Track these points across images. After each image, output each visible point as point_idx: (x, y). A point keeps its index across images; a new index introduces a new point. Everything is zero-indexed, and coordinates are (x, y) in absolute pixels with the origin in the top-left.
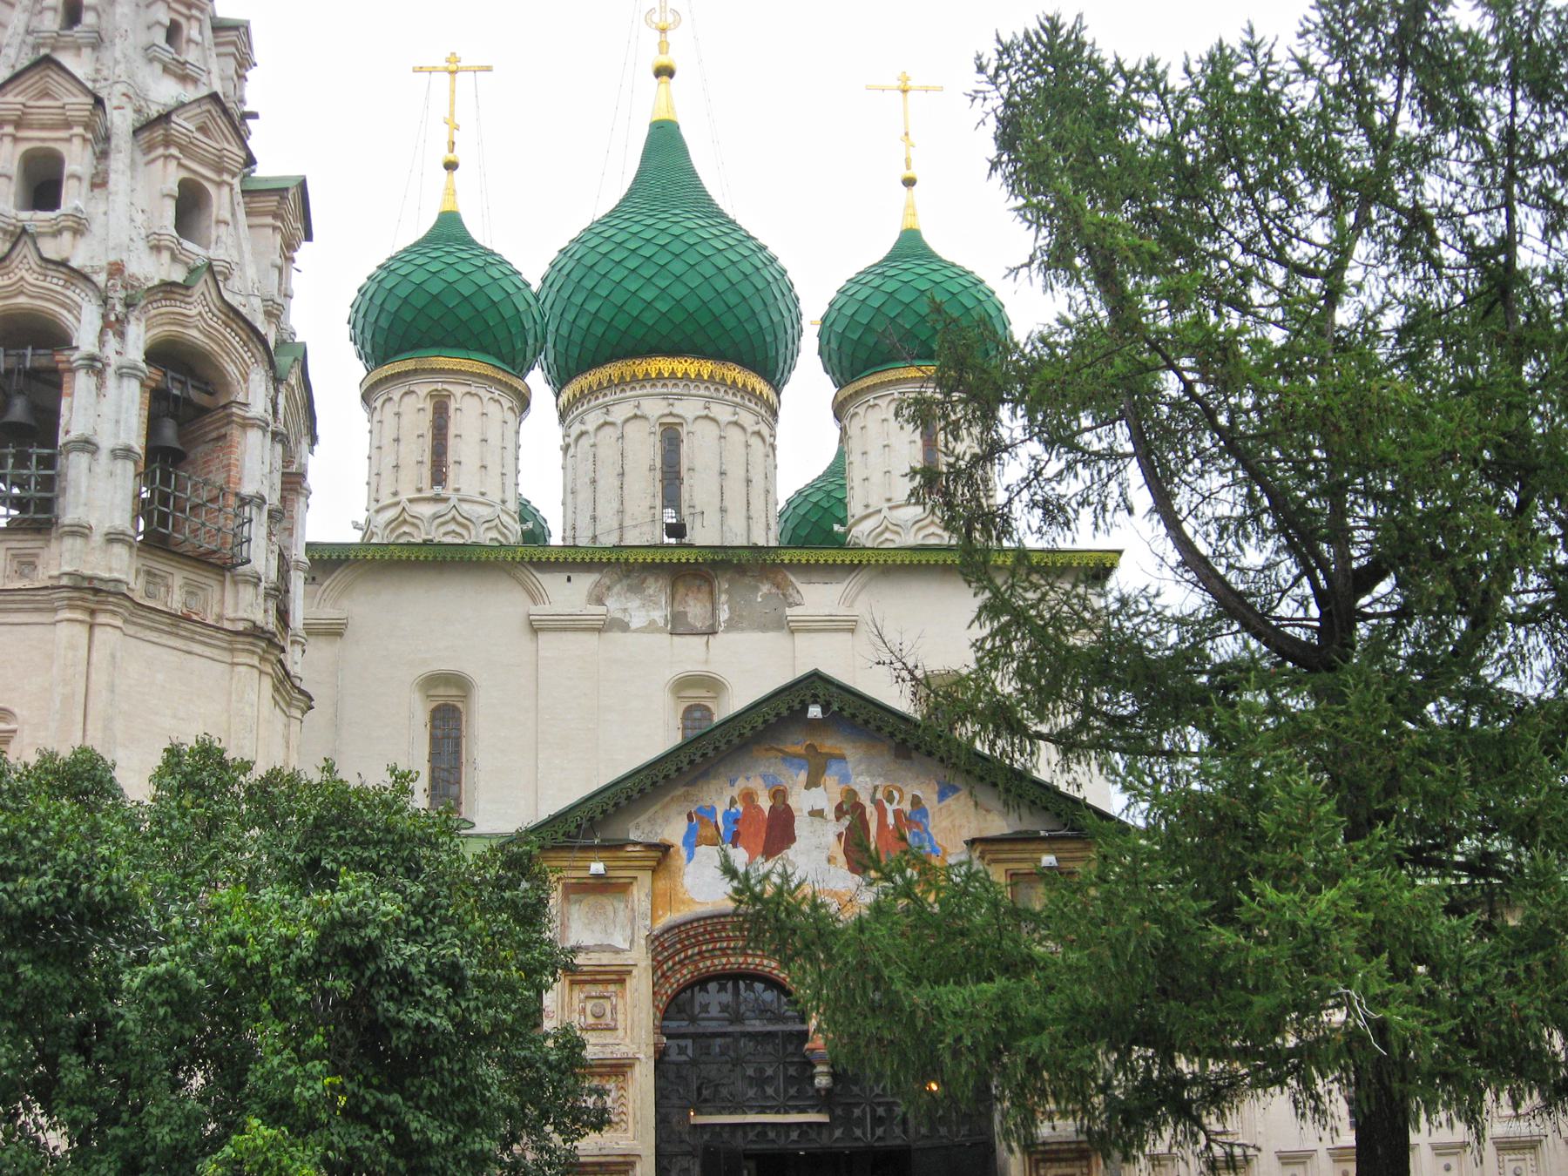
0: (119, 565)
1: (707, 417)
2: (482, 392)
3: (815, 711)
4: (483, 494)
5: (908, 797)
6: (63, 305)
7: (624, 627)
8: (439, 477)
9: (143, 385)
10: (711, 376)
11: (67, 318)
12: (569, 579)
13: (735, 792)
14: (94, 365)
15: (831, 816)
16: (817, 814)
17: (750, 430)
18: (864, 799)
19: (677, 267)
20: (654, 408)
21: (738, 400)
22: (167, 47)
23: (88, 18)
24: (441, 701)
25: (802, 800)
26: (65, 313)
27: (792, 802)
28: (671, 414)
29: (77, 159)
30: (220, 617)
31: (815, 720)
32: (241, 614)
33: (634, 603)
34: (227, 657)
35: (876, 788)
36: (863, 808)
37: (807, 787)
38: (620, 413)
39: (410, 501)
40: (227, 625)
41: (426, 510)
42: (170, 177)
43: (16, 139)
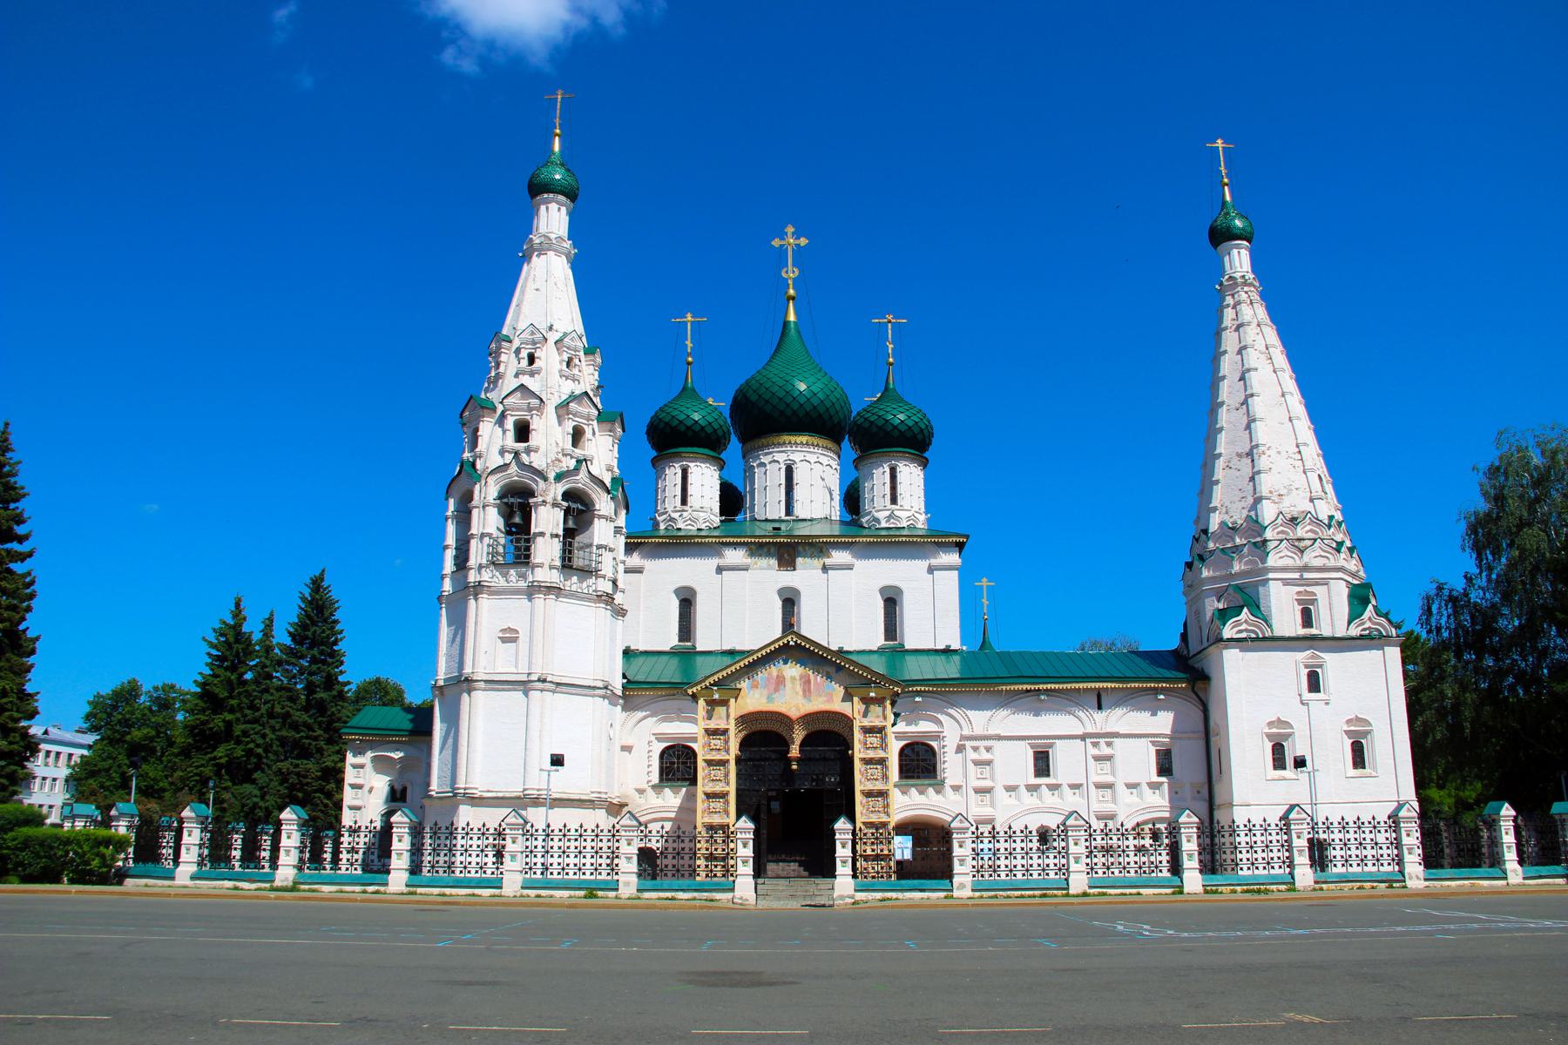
0: (554, 577)
4: (702, 508)
8: (684, 501)
15: (798, 678)
16: (793, 679)
17: (825, 464)
20: (781, 457)
22: (567, 370)
27: (785, 674)
37: (790, 668)
42: (569, 426)
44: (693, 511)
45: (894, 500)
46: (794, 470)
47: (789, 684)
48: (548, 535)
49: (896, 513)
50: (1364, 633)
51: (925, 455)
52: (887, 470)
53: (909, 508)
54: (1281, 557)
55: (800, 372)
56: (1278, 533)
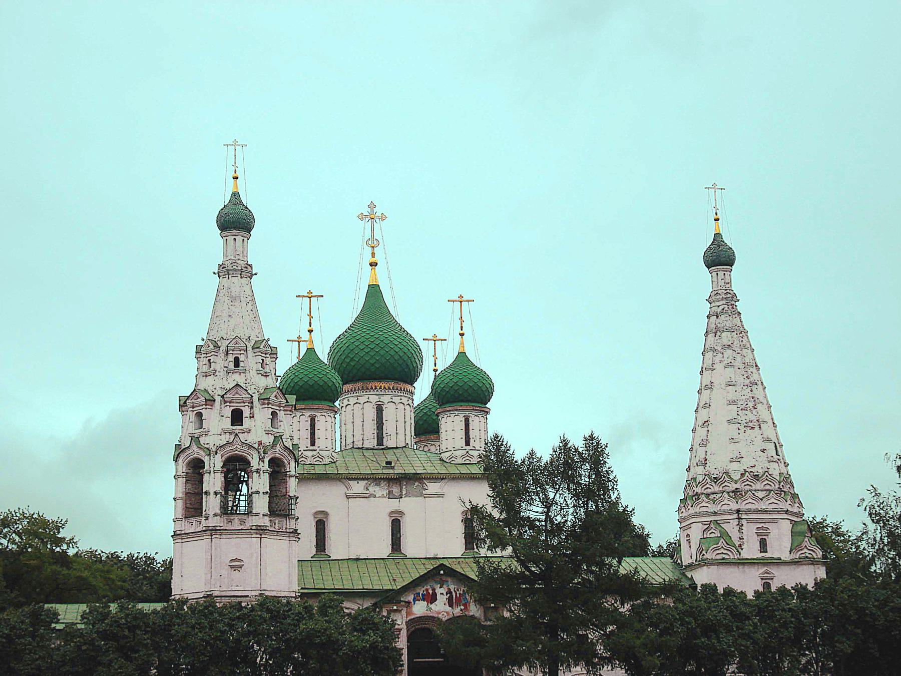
0: (266, 521)
1: (392, 402)
2: (325, 414)
3: (442, 572)
5: (462, 590)
6: (248, 454)
7: (375, 496)
8: (313, 444)
9: (269, 473)
10: (393, 388)
11: (249, 458)
12: (358, 483)
13: (424, 589)
14: (258, 471)
15: (445, 594)
18: (452, 590)
19: (382, 352)
20: (374, 399)
21: (402, 394)
23: (241, 364)
24: (318, 519)
25: (439, 591)
26: (248, 456)
28: (380, 401)
29: (246, 412)
30: (286, 528)
31: (442, 574)
32: (291, 527)
33: (377, 488)
34: (288, 539)
35: (455, 588)
36: (452, 592)
38: (362, 400)
39: (304, 450)
40: (288, 531)
41: (309, 454)
43: (230, 406)
44: (320, 450)
45: (467, 443)
46: (384, 408)
47: (438, 596)
48: (261, 493)
49: (470, 452)
50: (801, 556)
51: (487, 406)
52: (463, 419)
53: (480, 449)
54: (747, 504)
55: (385, 328)
56: (745, 485)
